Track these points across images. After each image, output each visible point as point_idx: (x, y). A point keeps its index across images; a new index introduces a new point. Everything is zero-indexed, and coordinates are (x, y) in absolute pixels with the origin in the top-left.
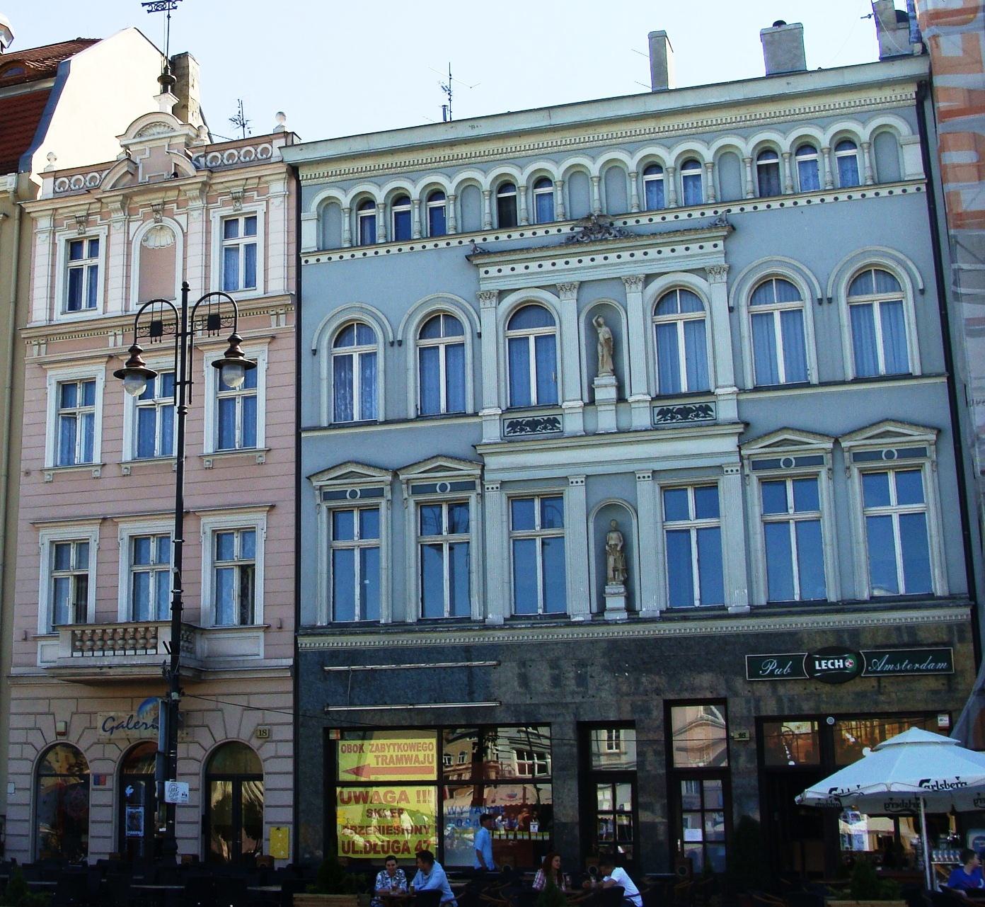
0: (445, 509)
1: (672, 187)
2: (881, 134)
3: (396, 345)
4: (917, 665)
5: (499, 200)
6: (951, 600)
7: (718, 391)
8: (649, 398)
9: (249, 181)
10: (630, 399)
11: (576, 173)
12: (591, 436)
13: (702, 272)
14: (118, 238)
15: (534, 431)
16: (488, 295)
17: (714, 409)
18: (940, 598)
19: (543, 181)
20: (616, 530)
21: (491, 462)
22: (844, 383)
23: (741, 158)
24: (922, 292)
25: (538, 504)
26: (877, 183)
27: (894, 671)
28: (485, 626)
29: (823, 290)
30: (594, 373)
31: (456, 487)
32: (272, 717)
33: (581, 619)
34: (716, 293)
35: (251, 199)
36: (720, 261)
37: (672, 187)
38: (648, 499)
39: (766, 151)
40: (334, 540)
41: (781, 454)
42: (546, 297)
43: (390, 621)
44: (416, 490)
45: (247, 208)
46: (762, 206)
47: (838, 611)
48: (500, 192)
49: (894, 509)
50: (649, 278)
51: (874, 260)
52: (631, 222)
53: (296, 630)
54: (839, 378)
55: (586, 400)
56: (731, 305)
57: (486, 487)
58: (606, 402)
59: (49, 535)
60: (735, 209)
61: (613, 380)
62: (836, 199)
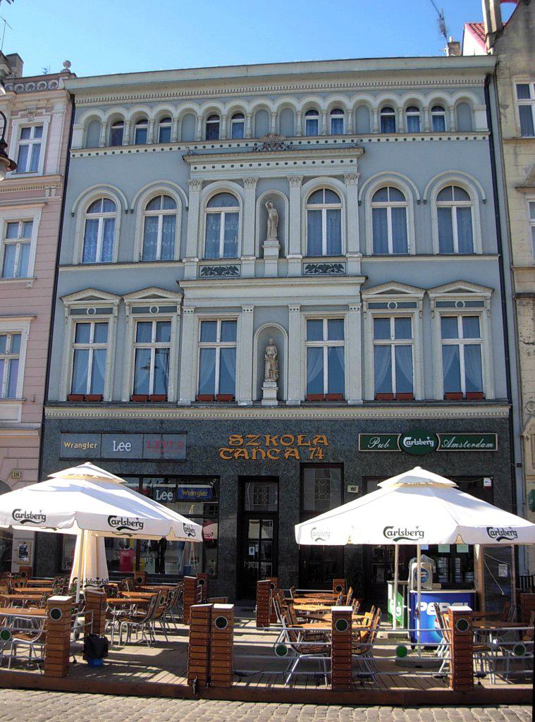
0: (155, 326)
1: (324, 122)
2: (463, 104)
3: (129, 212)
4: (474, 445)
5: (208, 125)
6: (496, 402)
7: (348, 255)
8: (301, 257)
9: (41, 102)
10: (288, 257)
11: (262, 111)
13: (341, 178)
15: (220, 274)
16: (195, 183)
17: (344, 267)
18: (489, 400)
19: (238, 115)
20: (273, 345)
21: (188, 293)
22: (432, 255)
23: (370, 110)
24: (485, 201)
25: (218, 326)
26: (459, 131)
27: (459, 448)
28: (176, 405)
29: (421, 196)
30: (264, 237)
31: (163, 310)
32: (23, 464)
33: (245, 404)
34: (349, 192)
35: (41, 114)
37: (324, 122)
38: (297, 324)
39: (387, 108)
40: (75, 342)
41: (388, 299)
42: (235, 187)
43: (110, 400)
44: (135, 310)
45: (37, 120)
46: (383, 139)
47: (422, 406)
48: (208, 120)
50: (306, 180)
51: (455, 178)
52: (296, 143)
53: (44, 404)
54: (428, 252)
55: (257, 254)
56: (360, 200)
57: (184, 310)
58: (271, 257)
60: (366, 140)
61: (277, 242)
62: (432, 139)
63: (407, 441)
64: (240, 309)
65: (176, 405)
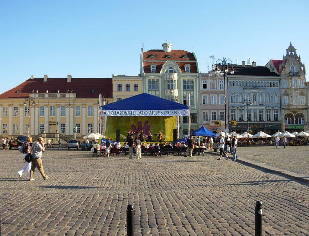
2: (277, 82)
12: (254, 106)
13: (263, 93)
14: (209, 82)
28: (245, 121)
31: (243, 109)
36: (264, 92)
49: (276, 114)
59: (203, 111)
63: (271, 126)
64: (251, 109)
65: (245, 121)
